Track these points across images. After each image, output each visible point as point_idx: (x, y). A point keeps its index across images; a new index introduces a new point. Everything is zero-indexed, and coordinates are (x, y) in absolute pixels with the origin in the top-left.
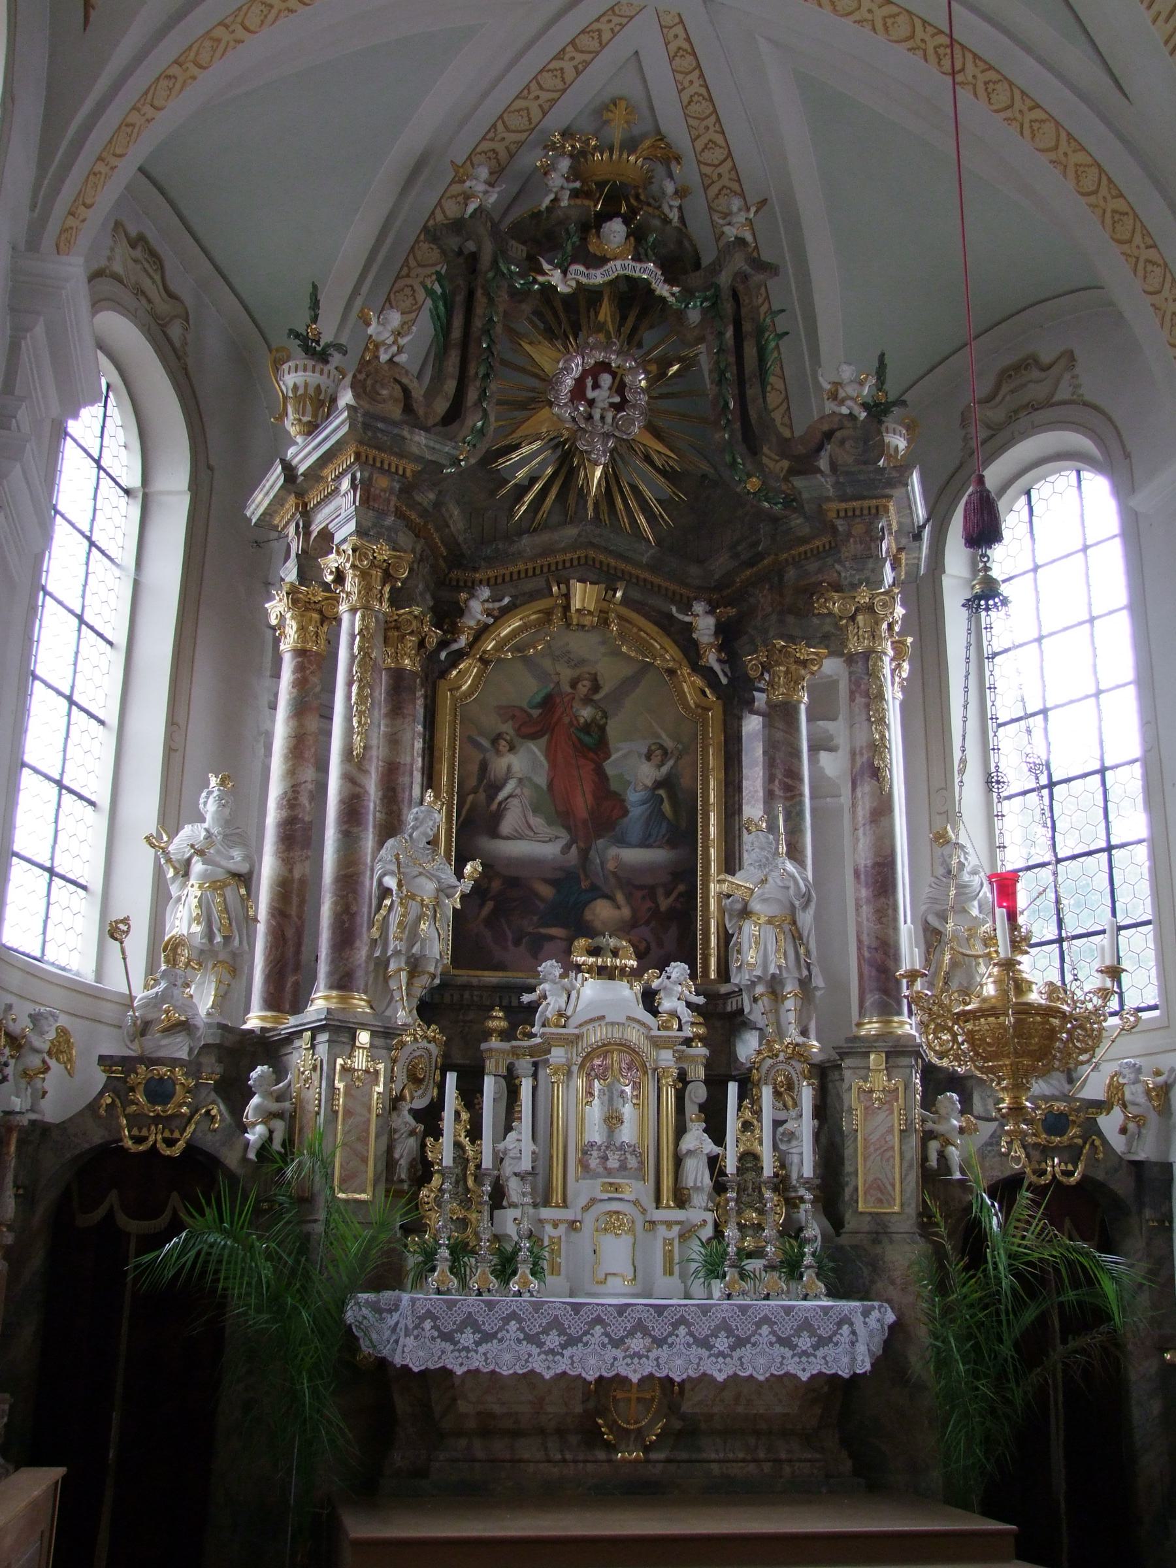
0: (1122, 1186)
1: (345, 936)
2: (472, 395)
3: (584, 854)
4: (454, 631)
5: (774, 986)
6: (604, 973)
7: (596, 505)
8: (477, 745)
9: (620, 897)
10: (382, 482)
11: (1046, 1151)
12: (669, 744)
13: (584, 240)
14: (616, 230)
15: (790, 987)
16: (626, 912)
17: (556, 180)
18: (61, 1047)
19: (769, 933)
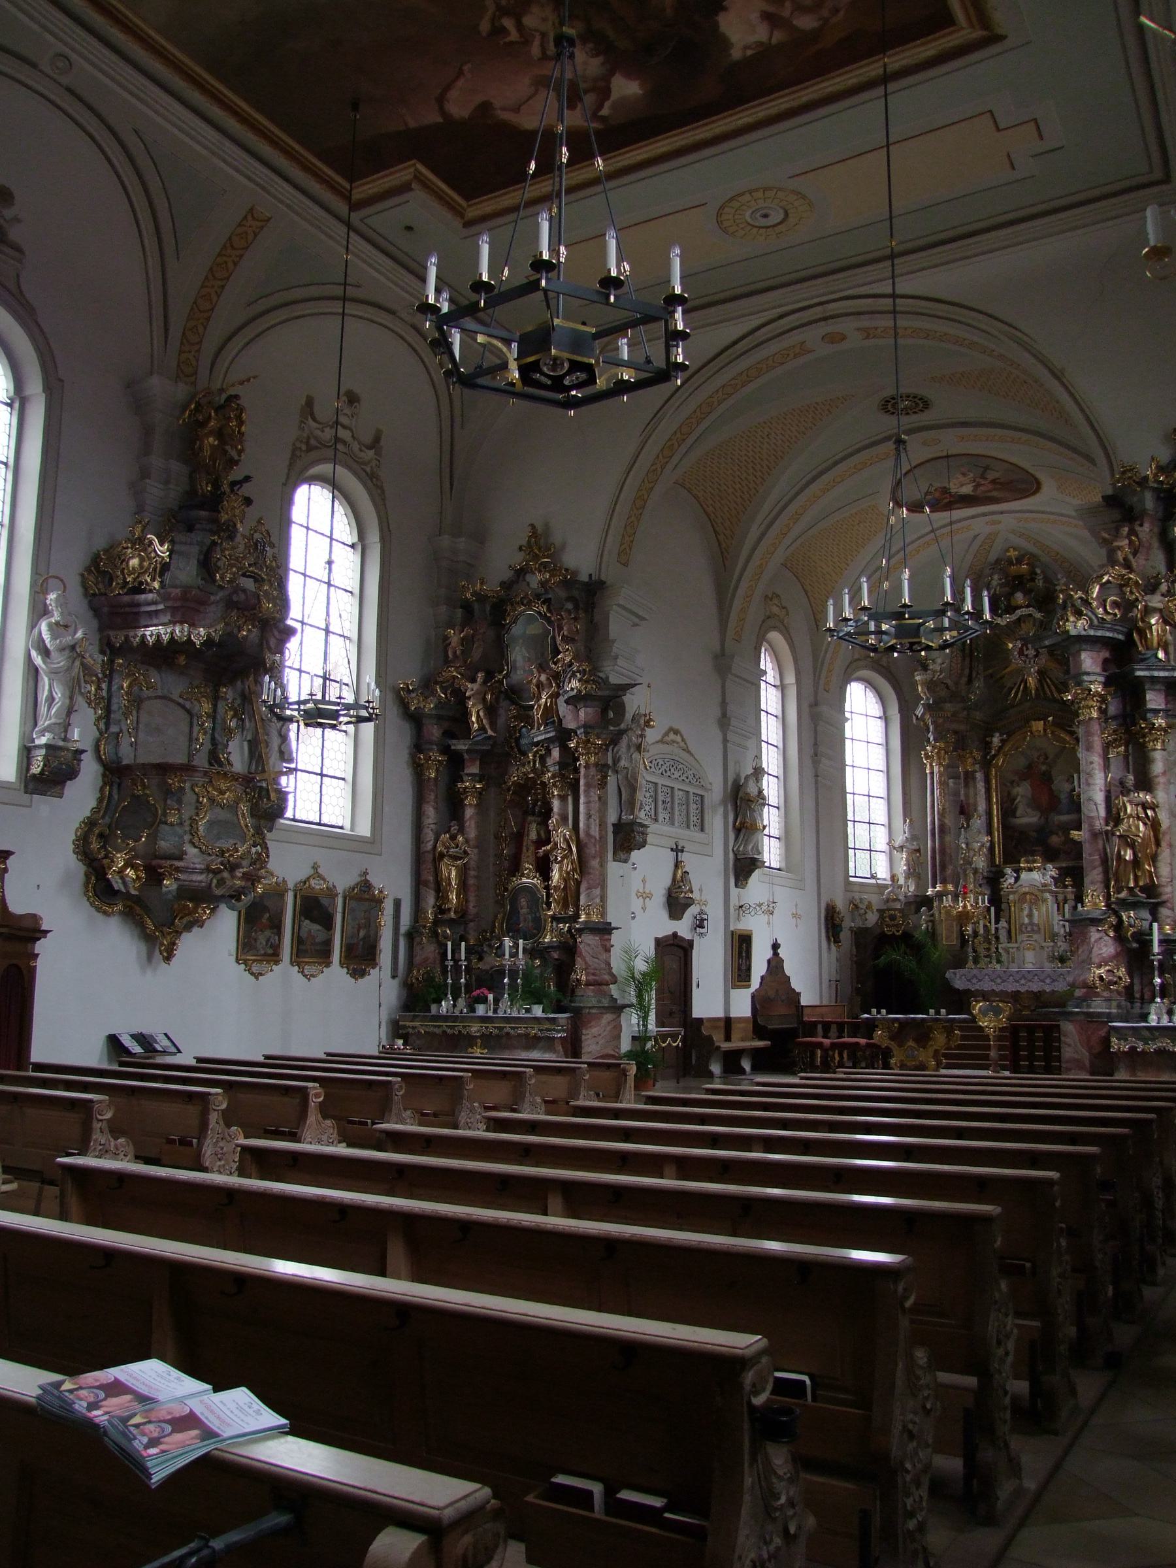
2: (974, 675)
4: (990, 749)
6: (1030, 870)
7: (1037, 690)
8: (1005, 785)
9: (1060, 834)
10: (941, 720)
13: (1009, 600)
14: (1019, 598)
16: (1063, 838)
18: (869, 906)
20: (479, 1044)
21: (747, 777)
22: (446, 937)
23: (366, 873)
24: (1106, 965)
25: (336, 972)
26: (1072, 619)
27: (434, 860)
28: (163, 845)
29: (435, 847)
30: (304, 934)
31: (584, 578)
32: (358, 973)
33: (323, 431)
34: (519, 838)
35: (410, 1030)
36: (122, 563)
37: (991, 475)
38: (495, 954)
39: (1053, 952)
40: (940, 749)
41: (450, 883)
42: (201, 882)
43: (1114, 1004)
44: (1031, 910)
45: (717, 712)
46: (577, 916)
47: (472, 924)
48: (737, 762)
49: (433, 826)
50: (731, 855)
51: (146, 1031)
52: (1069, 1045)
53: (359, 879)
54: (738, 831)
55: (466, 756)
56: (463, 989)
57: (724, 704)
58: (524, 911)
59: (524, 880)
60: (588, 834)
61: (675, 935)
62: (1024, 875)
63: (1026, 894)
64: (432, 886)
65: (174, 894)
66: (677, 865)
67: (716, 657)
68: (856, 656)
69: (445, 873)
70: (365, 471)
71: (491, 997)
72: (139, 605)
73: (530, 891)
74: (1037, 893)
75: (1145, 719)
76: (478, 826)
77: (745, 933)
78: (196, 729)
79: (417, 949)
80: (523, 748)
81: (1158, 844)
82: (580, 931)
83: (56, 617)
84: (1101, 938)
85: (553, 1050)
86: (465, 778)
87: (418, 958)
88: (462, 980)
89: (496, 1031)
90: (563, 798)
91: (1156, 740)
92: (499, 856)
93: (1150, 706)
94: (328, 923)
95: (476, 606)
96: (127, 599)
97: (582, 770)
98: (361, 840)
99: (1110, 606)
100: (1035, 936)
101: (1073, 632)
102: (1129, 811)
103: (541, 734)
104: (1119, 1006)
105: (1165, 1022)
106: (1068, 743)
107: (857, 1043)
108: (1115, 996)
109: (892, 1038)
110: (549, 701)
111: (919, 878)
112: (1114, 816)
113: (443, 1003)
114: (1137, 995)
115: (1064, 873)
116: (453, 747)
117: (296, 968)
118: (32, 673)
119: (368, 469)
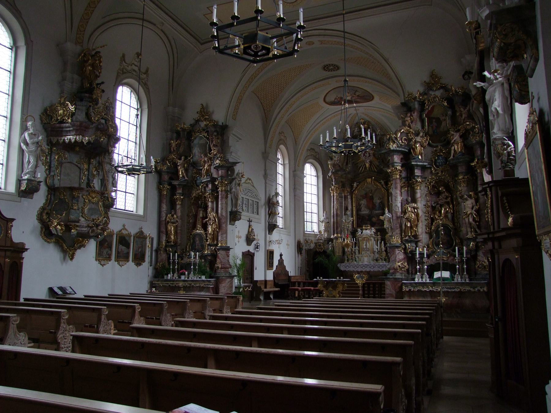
1: (337, 229)
2: (348, 162)
3: (371, 212)
5: (388, 228)
6: (366, 229)
7: (369, 168)
10: (337, 178)
12: (381, 197)
15: (390, 229)
16: (377, 219)
17: (356, 131)
18: (312, 241)
19: (387, 222)
20: (182, 290)
21: (273, 196)
22: (169, 251)
23: (141, 228)
24: (401, 262)
25: (131, 264)
26: (392, 144)
27: (166, 224)
28: (72, 217)
29: (166, 219)
30: (120, 250)
31: (220, 124)
32: (138, 264)
33: (128, 67)
34: (196, 216)
35: (157, 285)
36: (56, 112)
37: (357, 94)
38: (188, 257)
39: (374, 257)
40: (337, 187)
41: (171, 232)
42: (86, 231)
43: (403, 275)
44: (366, 243)
45: (263, 172)
46: (217, 245)
47: (179, 247)
48: (269, 190)
49: (165, 211)
50: (267, 223)
51: (63, 286)
52: (388, 289)
53: (139, 230)
54: (270, 215)
55: (177, 187)
56: (176, 270)
57: (265, 170)
58: (198, 242)
59: (198, 231)
60: (222, 215)
61: (249, 251)
62: (364, 231)
63: (365, 238)
64: (165, 233)
65: (76, 235)
66: (250, 226)
67: (263, 153)
68: (308, 154)
69: (169, 228)
70: (142, 82)
71: (186, 273)
72: (63, 128)
73: (200, 235)
74: (369, 237)
75: (414, 179)
76: (181, 212)
77: (271, 250)
78: (82, 174)
79: (159, 255)
80: (198, 184)
81: (418, 221)
82: (219, 249)
83: (31, 131)
84: (399, 253)
85: (209, 291)
86: (177, 194)
87: (159, 259)
88: (176, 267)
89: (188, 285)
90: (212, 202)
91: (418, 186)
92: (189, 222)
93: (416, 174)
94: (128, 246)
95: (181, 132)
96: (58, 125)
97: (220, 192)
98: (139, 216)
99: (404, 141)
100: (368, 252)
101: (392, 149)
102: (409, 210)
103: (205, 179)
104: (405, 276)
105: (420, 281)
106: (378, 186)
107: (311, 289)
108: (403, 272)
109: (324, 287)
110: (208, 167)
111: (329, 232)
112: (404, 212)
113: (169, 275)
114: (410, 272)
115: (377, 231)
116: (173, 183)
117: (117, 262)
118: (21, 151)
119: (144, 82)
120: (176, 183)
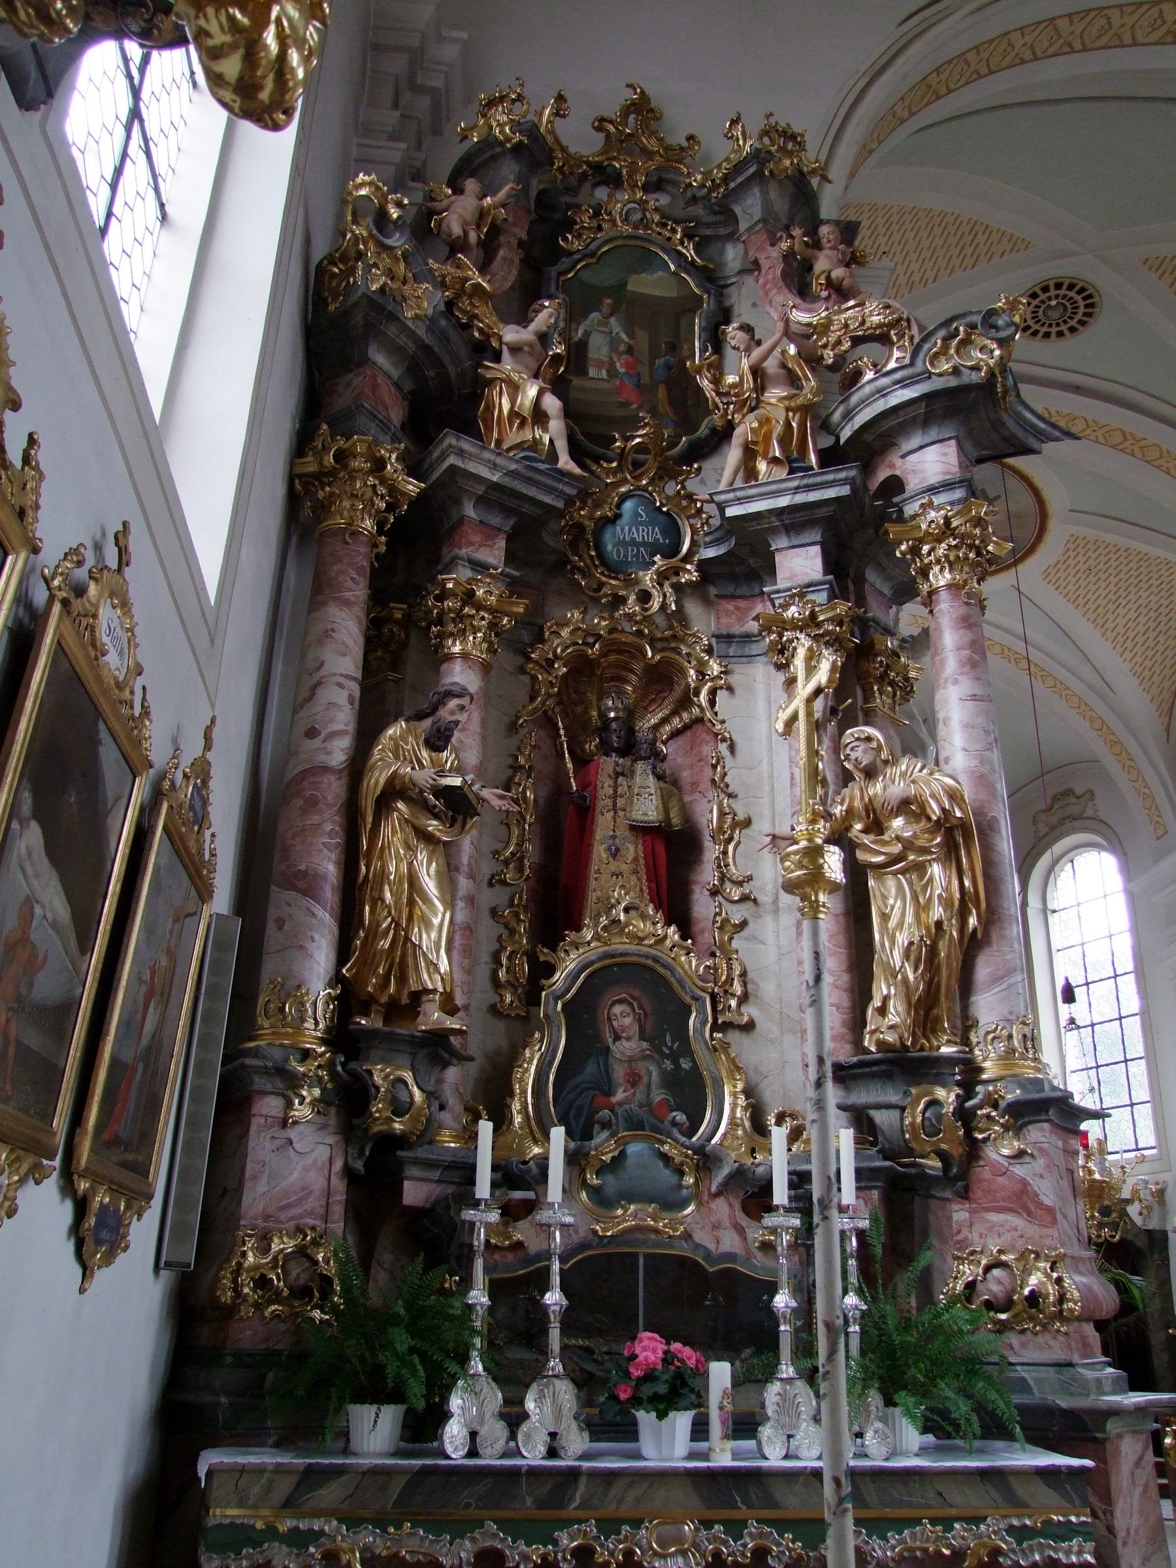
0: (1142, 1242)
11: (1101, 1226)
55: (470, 511)
58: (628, 1047)
87: (262, 1187)
120: (485, 473)
